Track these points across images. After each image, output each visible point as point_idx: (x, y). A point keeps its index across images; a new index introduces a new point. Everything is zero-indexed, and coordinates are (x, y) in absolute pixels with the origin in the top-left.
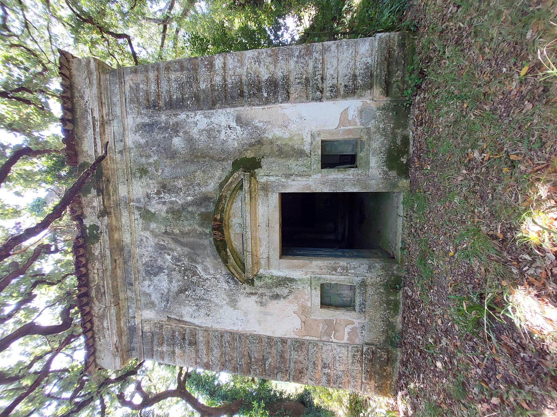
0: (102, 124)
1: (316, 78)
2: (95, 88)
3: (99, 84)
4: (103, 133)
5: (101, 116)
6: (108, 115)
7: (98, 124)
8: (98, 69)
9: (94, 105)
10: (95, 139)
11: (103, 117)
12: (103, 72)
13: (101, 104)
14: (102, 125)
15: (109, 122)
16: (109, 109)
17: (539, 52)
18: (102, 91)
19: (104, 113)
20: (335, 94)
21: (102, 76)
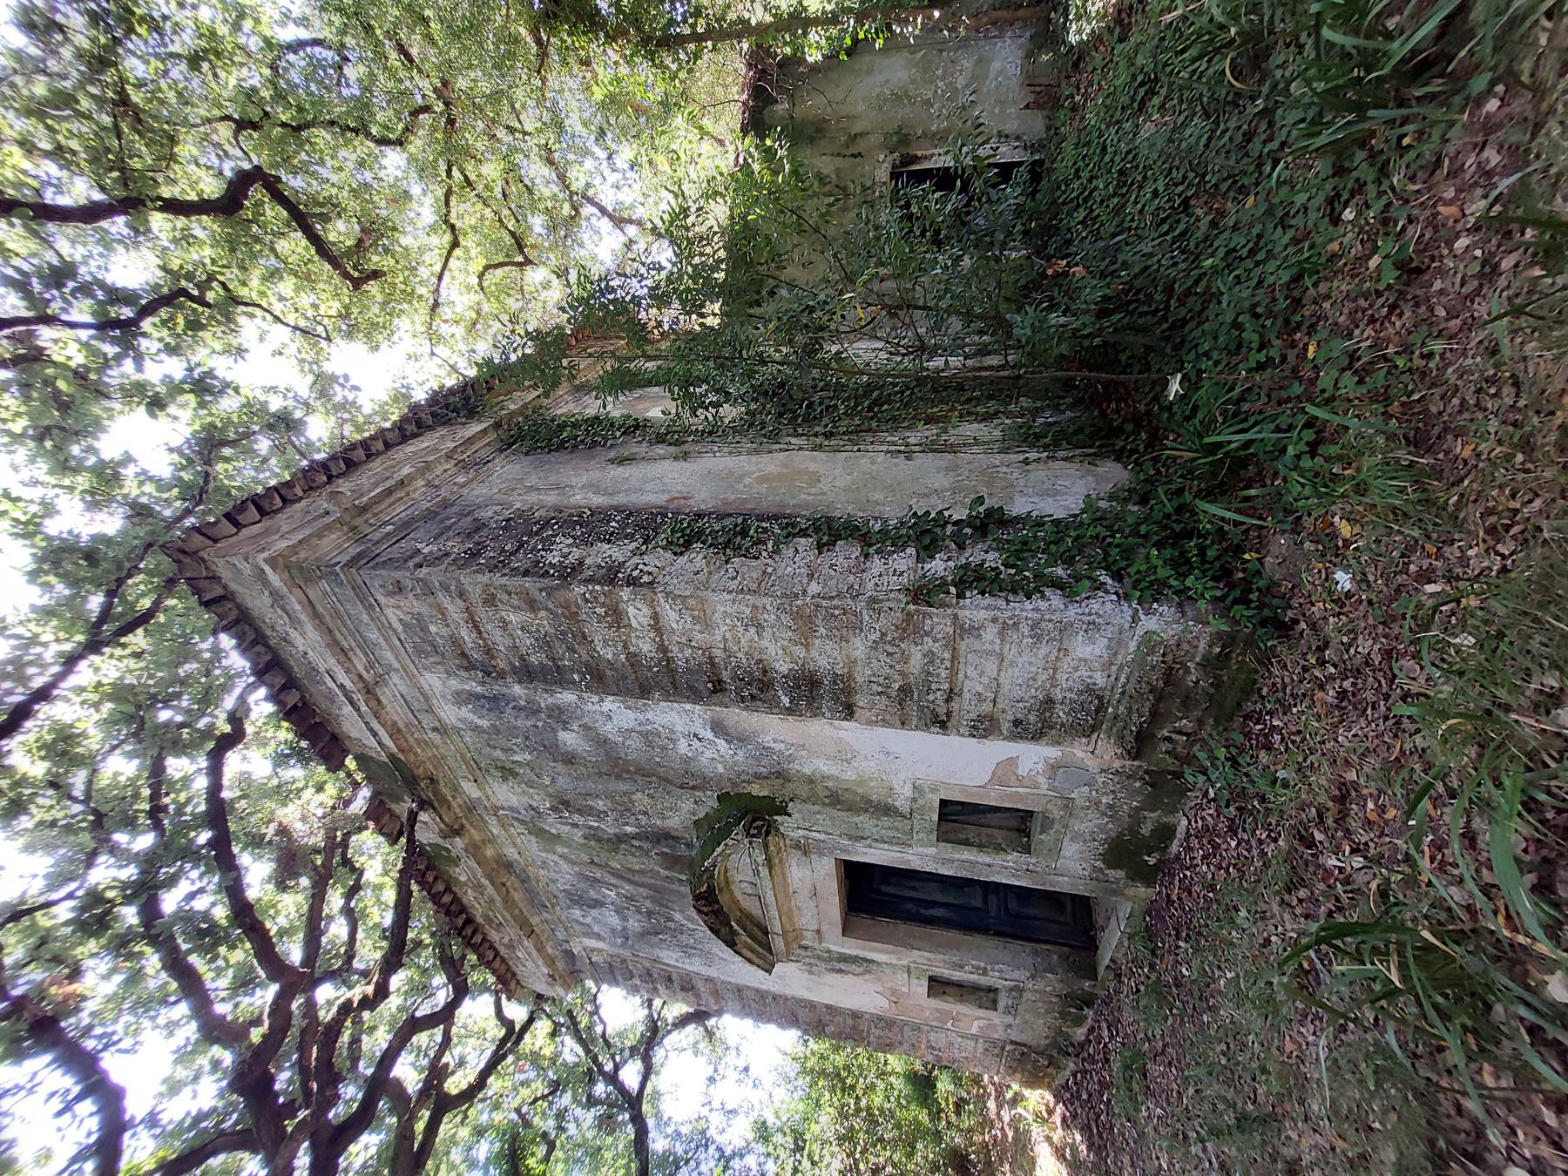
0: (368, 692)
1: (931, 698)
2: (309, 628)
3: (316, 615)
4: (378, 709)
5: (356, 679)
6: (370, 666)
7: (359, 698)
8: (292, 583)
9: (325, 661)
10: (366, 723)
11: (360, 676)
12: (307, 580)
13: (343, 654)
14: (369, 691)
15: (380, 680)
16: (366, 654)
17: (1168, 17)
18: (331, 625)
19: (361, 668)
20: (983, 727)
21: (311, 593)
